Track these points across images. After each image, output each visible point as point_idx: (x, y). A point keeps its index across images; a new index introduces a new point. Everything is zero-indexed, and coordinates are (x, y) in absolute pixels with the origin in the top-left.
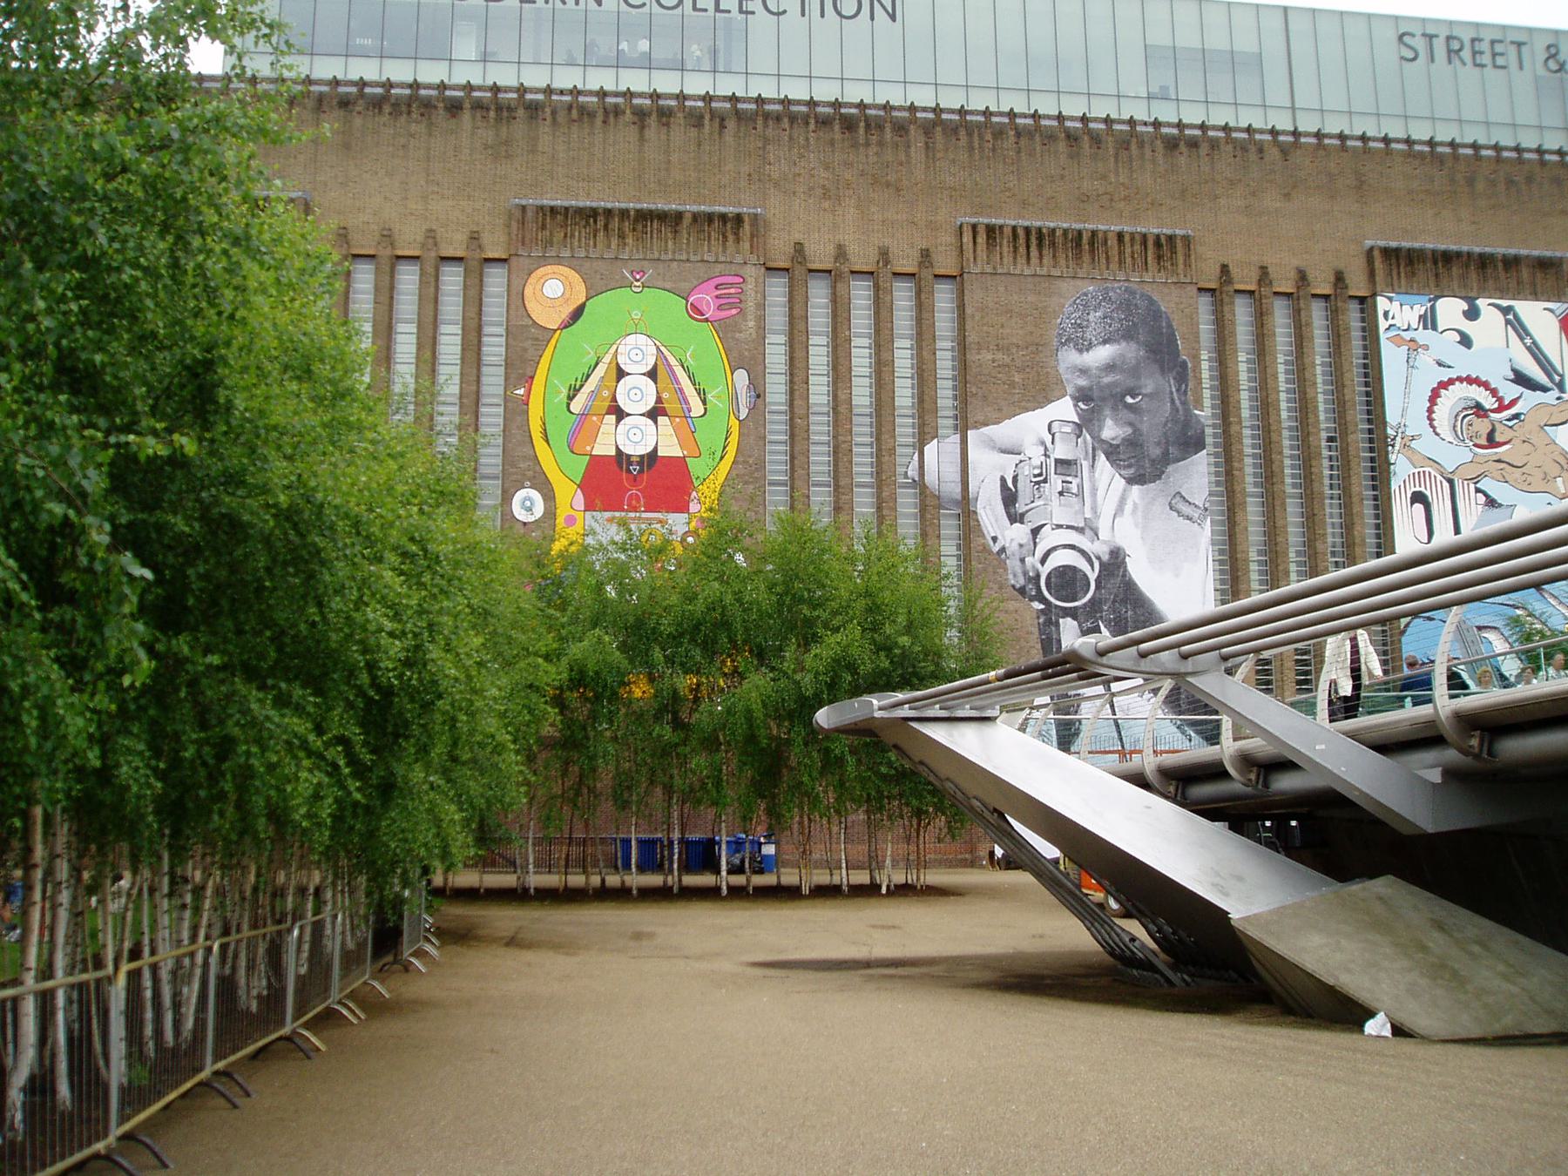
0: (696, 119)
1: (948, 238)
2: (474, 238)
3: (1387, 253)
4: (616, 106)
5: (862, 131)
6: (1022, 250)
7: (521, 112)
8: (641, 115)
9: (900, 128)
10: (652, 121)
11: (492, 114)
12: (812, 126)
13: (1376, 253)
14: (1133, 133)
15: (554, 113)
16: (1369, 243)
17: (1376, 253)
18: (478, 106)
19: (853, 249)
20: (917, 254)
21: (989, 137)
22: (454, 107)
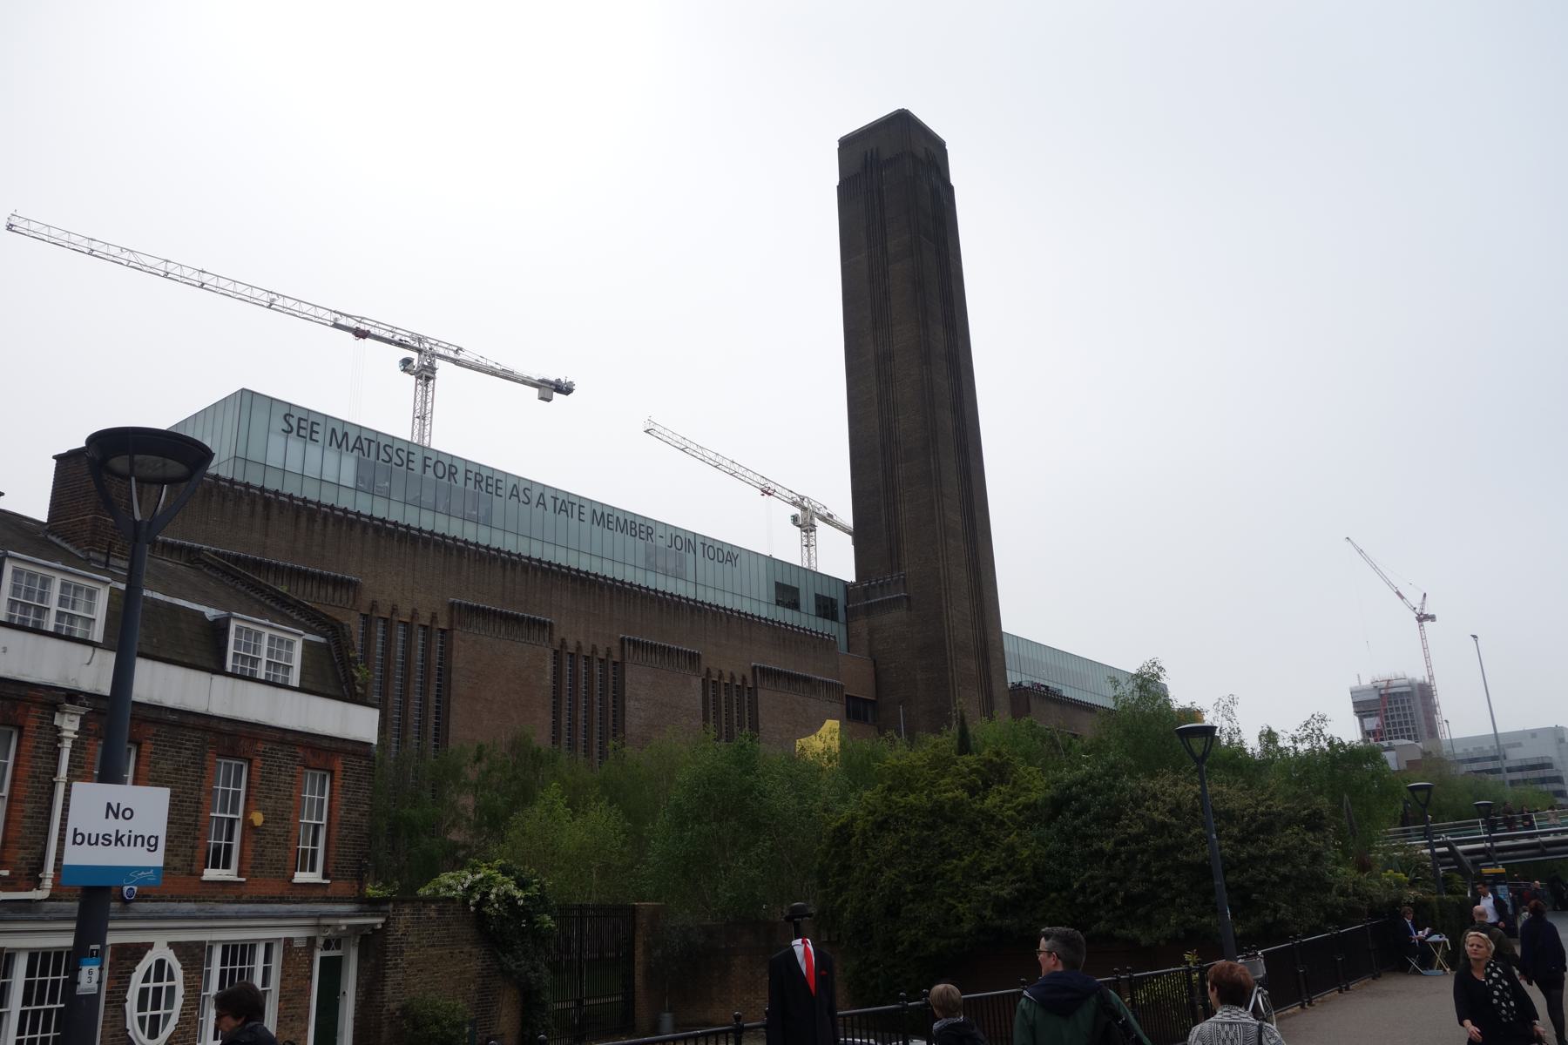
0: (525, 568)
1: (617, 644)
2: (434, 617)
3: (762, 670)
4: (495, 555)
5: (587, 587)
6: (645, 650)
7: (455, 552)
8: (504, 561)
9: (601, 586)
10: (509, 566)
11: (443, 550)
12: (569, 581)
13: (758, 670)
14: (680, 602)
15: (469, 555)
16: (753, 664)
17: (758, 670)
18: (436, 544)
19: (583, 644)
20: (605, 650)
21: (632, 597)
22: (426, 542)
